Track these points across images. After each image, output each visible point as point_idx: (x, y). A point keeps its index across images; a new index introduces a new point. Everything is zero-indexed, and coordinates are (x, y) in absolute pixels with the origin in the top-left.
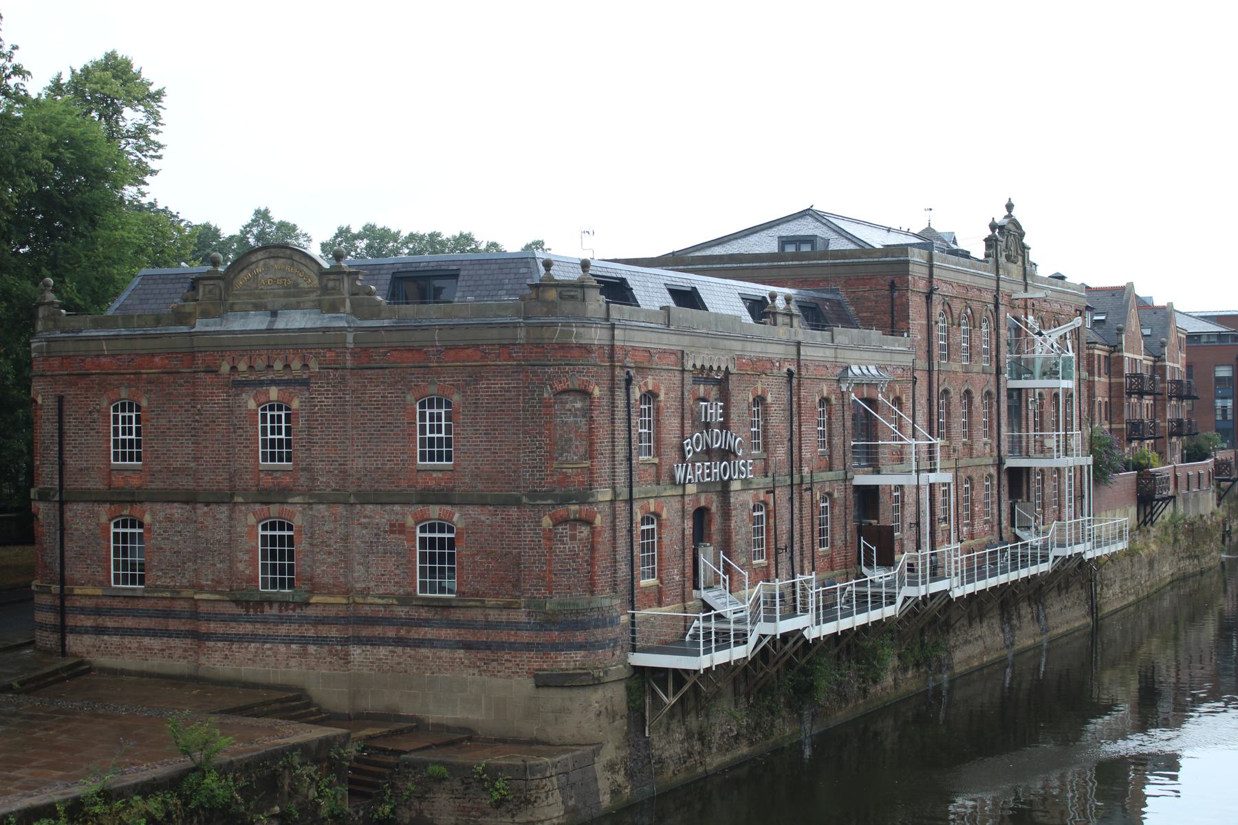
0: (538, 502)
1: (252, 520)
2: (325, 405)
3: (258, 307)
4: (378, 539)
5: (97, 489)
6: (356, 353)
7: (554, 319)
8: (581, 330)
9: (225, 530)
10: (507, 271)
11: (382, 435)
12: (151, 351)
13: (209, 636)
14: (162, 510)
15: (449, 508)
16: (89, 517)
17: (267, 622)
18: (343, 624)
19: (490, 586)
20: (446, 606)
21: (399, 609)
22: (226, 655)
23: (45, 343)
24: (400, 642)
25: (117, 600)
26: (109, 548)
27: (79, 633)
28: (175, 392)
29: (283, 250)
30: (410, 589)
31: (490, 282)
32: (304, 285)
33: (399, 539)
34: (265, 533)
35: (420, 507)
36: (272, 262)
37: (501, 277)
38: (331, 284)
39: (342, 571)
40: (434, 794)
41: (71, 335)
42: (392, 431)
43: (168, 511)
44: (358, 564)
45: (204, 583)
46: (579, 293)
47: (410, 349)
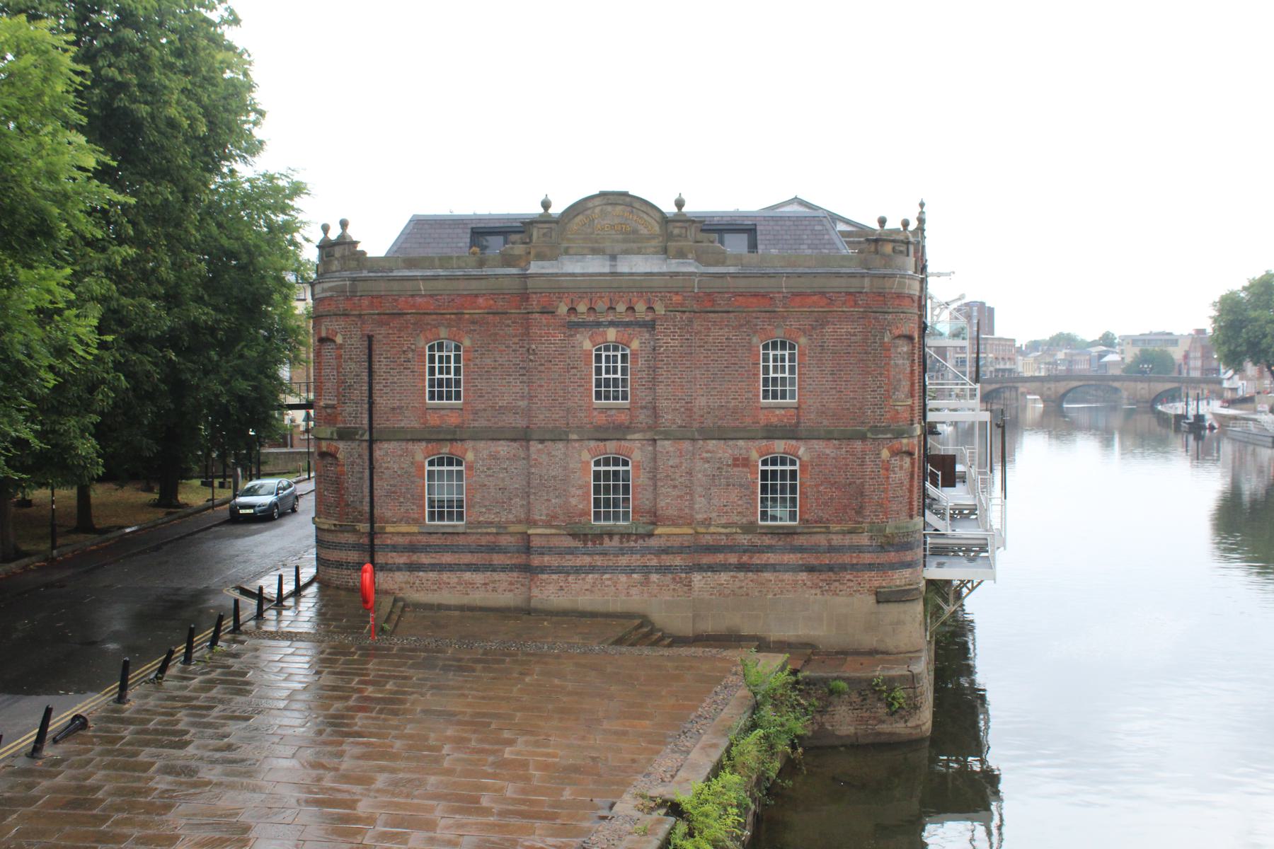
0: (880, 436)
1: (586, 456)
2: (671, 346)
3: (595, 251)
4: (720, 472)
5: (411, 428)
6: (699, 297)
7: (889, 271)
8: (911, 282)
9: (560, 466)
10: (804, 227)
11: (726, 374)
12: (475, 292)
13: (543, 569)
14: (485, 448)
15: (794, 442)
16: (402, 456)
17: (606, 554)
18: (687, 553)
19: (833, 513)
20: (789, 533)
21: (742, 537)
22: (561, 587)
23: (348, 283)
24: (742, 567)
25: (435, 536)
26: (424, 486)
27: (391, 570)
28: (501, 332)
29: (622, 198)
30: (752, 519)
31: (789, 237)
32: (644, 231)
33: (743, 472)
34: (432, 468)
35: (764, 443)
36: (609, 208)
37: (798, 232)
38: (676, 231)
39: (687, 503)
40: (834, 707)
41: (380, 274)
42: (737, 371)
43: (493, 449)
44: (700, 496)
45: (537, 517)
46: (903, 248)
47: (755, 295)
